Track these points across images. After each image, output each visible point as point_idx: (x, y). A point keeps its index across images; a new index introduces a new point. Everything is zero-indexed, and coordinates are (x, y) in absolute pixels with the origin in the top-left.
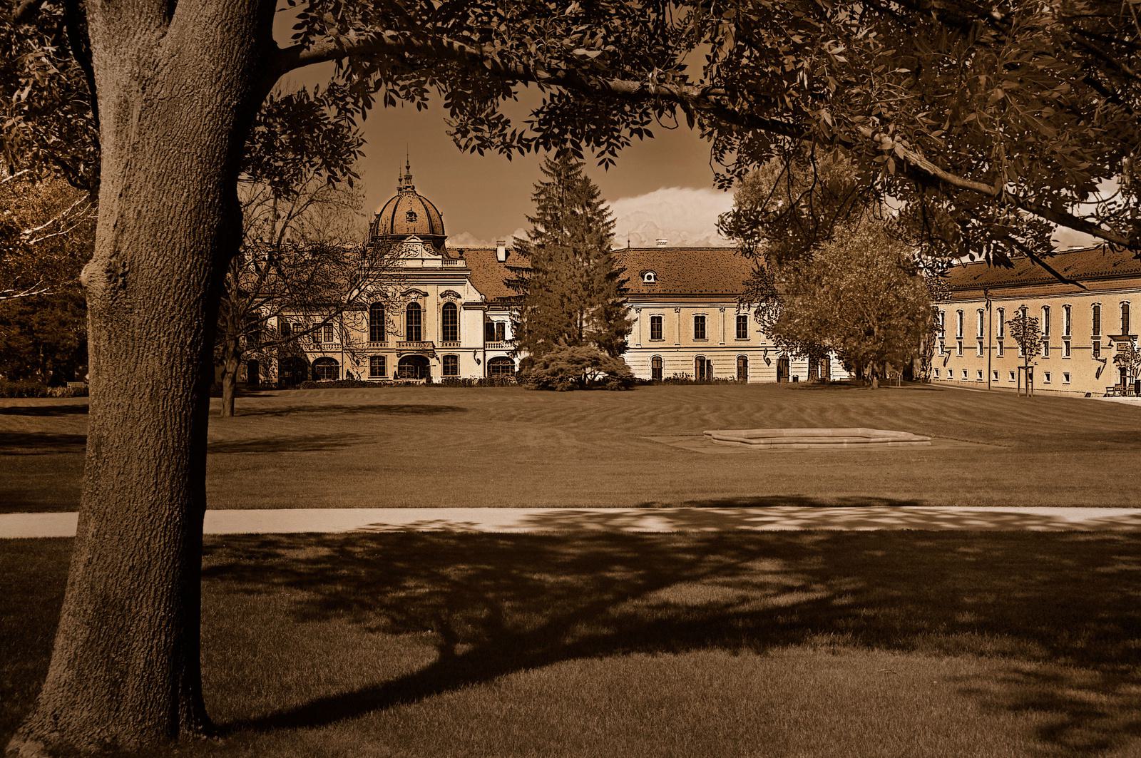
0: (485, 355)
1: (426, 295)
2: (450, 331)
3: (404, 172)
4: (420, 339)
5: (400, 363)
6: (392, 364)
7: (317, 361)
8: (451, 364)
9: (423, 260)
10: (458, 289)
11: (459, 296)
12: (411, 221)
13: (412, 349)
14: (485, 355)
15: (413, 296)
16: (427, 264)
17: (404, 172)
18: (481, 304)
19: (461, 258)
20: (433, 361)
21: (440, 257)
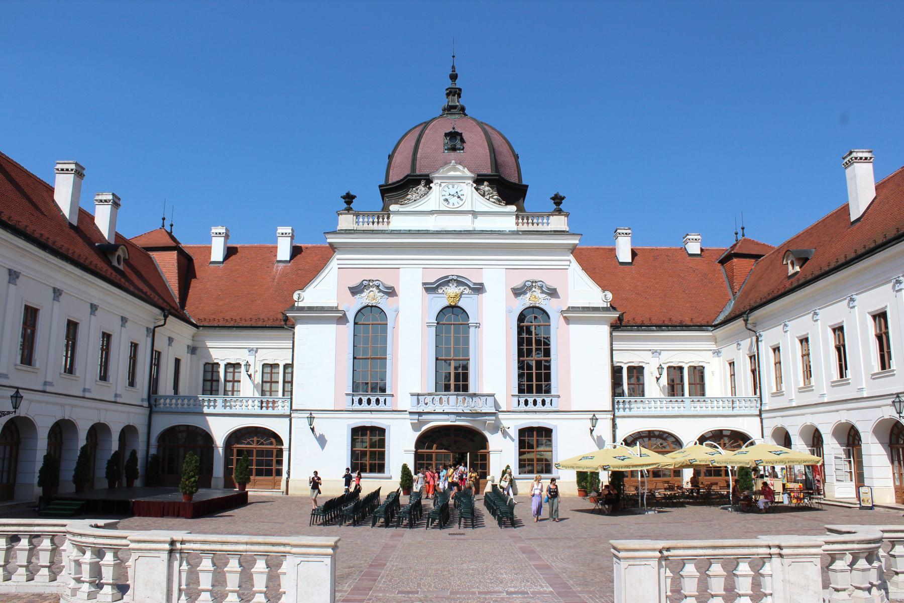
0: (614, 426)
1: (479, 289)
2: (535, 372)
3: (449, 84)
4: (466, 388)
5: (421, 442)
6: (400, 450)
7: (236, 436)
8: (534, 443)
9: (475, 214)
10: (551, 281)
11: (553, 293)
12: (454, 149)
13: (448, 410)
14: (614, 426)
15: (452, 290)
16: (483, 224)
17: (449, 84)
18: (604, 309)
19: (559, 212)
20: (494, 441)
21: (513, 208)
